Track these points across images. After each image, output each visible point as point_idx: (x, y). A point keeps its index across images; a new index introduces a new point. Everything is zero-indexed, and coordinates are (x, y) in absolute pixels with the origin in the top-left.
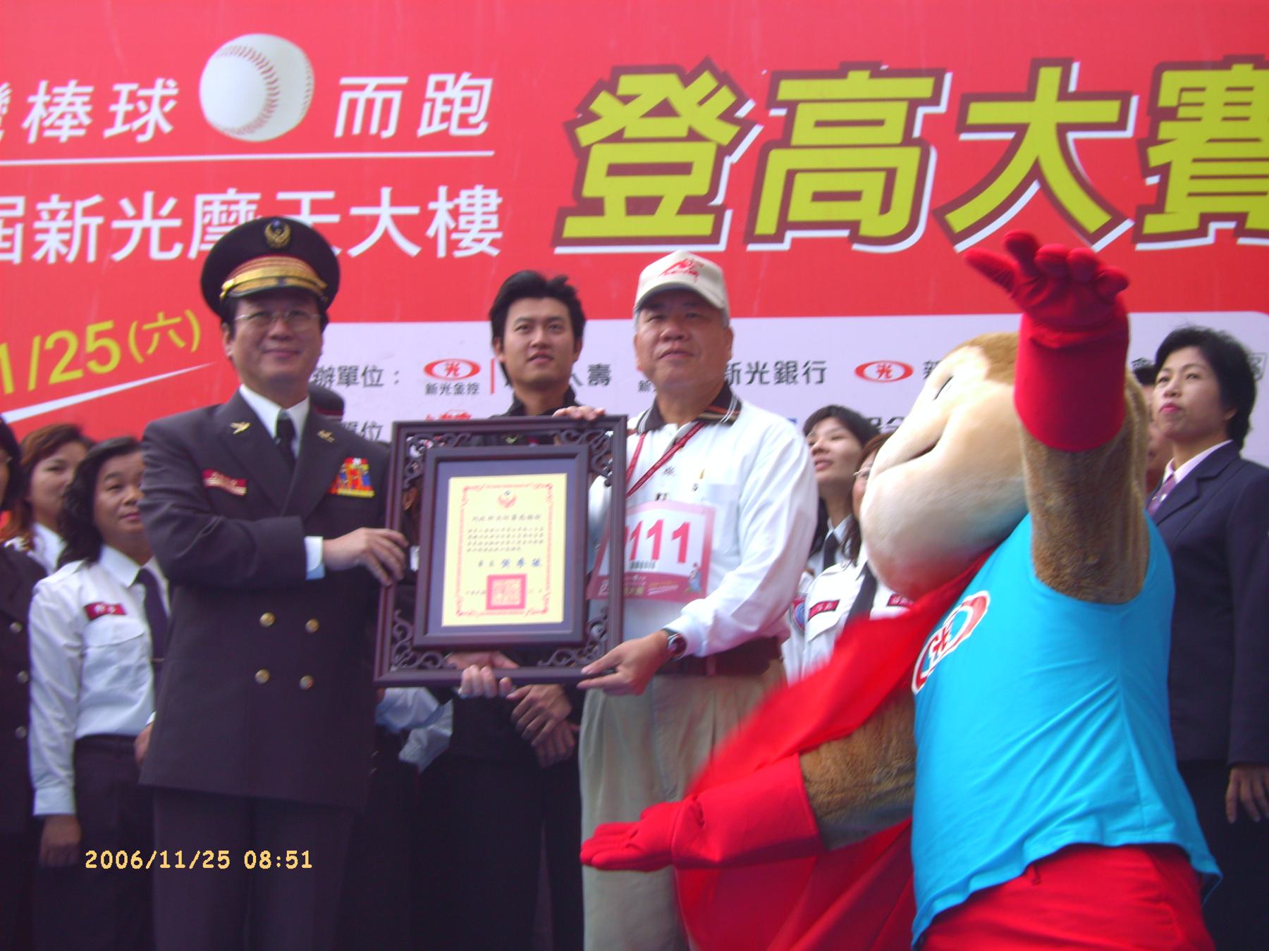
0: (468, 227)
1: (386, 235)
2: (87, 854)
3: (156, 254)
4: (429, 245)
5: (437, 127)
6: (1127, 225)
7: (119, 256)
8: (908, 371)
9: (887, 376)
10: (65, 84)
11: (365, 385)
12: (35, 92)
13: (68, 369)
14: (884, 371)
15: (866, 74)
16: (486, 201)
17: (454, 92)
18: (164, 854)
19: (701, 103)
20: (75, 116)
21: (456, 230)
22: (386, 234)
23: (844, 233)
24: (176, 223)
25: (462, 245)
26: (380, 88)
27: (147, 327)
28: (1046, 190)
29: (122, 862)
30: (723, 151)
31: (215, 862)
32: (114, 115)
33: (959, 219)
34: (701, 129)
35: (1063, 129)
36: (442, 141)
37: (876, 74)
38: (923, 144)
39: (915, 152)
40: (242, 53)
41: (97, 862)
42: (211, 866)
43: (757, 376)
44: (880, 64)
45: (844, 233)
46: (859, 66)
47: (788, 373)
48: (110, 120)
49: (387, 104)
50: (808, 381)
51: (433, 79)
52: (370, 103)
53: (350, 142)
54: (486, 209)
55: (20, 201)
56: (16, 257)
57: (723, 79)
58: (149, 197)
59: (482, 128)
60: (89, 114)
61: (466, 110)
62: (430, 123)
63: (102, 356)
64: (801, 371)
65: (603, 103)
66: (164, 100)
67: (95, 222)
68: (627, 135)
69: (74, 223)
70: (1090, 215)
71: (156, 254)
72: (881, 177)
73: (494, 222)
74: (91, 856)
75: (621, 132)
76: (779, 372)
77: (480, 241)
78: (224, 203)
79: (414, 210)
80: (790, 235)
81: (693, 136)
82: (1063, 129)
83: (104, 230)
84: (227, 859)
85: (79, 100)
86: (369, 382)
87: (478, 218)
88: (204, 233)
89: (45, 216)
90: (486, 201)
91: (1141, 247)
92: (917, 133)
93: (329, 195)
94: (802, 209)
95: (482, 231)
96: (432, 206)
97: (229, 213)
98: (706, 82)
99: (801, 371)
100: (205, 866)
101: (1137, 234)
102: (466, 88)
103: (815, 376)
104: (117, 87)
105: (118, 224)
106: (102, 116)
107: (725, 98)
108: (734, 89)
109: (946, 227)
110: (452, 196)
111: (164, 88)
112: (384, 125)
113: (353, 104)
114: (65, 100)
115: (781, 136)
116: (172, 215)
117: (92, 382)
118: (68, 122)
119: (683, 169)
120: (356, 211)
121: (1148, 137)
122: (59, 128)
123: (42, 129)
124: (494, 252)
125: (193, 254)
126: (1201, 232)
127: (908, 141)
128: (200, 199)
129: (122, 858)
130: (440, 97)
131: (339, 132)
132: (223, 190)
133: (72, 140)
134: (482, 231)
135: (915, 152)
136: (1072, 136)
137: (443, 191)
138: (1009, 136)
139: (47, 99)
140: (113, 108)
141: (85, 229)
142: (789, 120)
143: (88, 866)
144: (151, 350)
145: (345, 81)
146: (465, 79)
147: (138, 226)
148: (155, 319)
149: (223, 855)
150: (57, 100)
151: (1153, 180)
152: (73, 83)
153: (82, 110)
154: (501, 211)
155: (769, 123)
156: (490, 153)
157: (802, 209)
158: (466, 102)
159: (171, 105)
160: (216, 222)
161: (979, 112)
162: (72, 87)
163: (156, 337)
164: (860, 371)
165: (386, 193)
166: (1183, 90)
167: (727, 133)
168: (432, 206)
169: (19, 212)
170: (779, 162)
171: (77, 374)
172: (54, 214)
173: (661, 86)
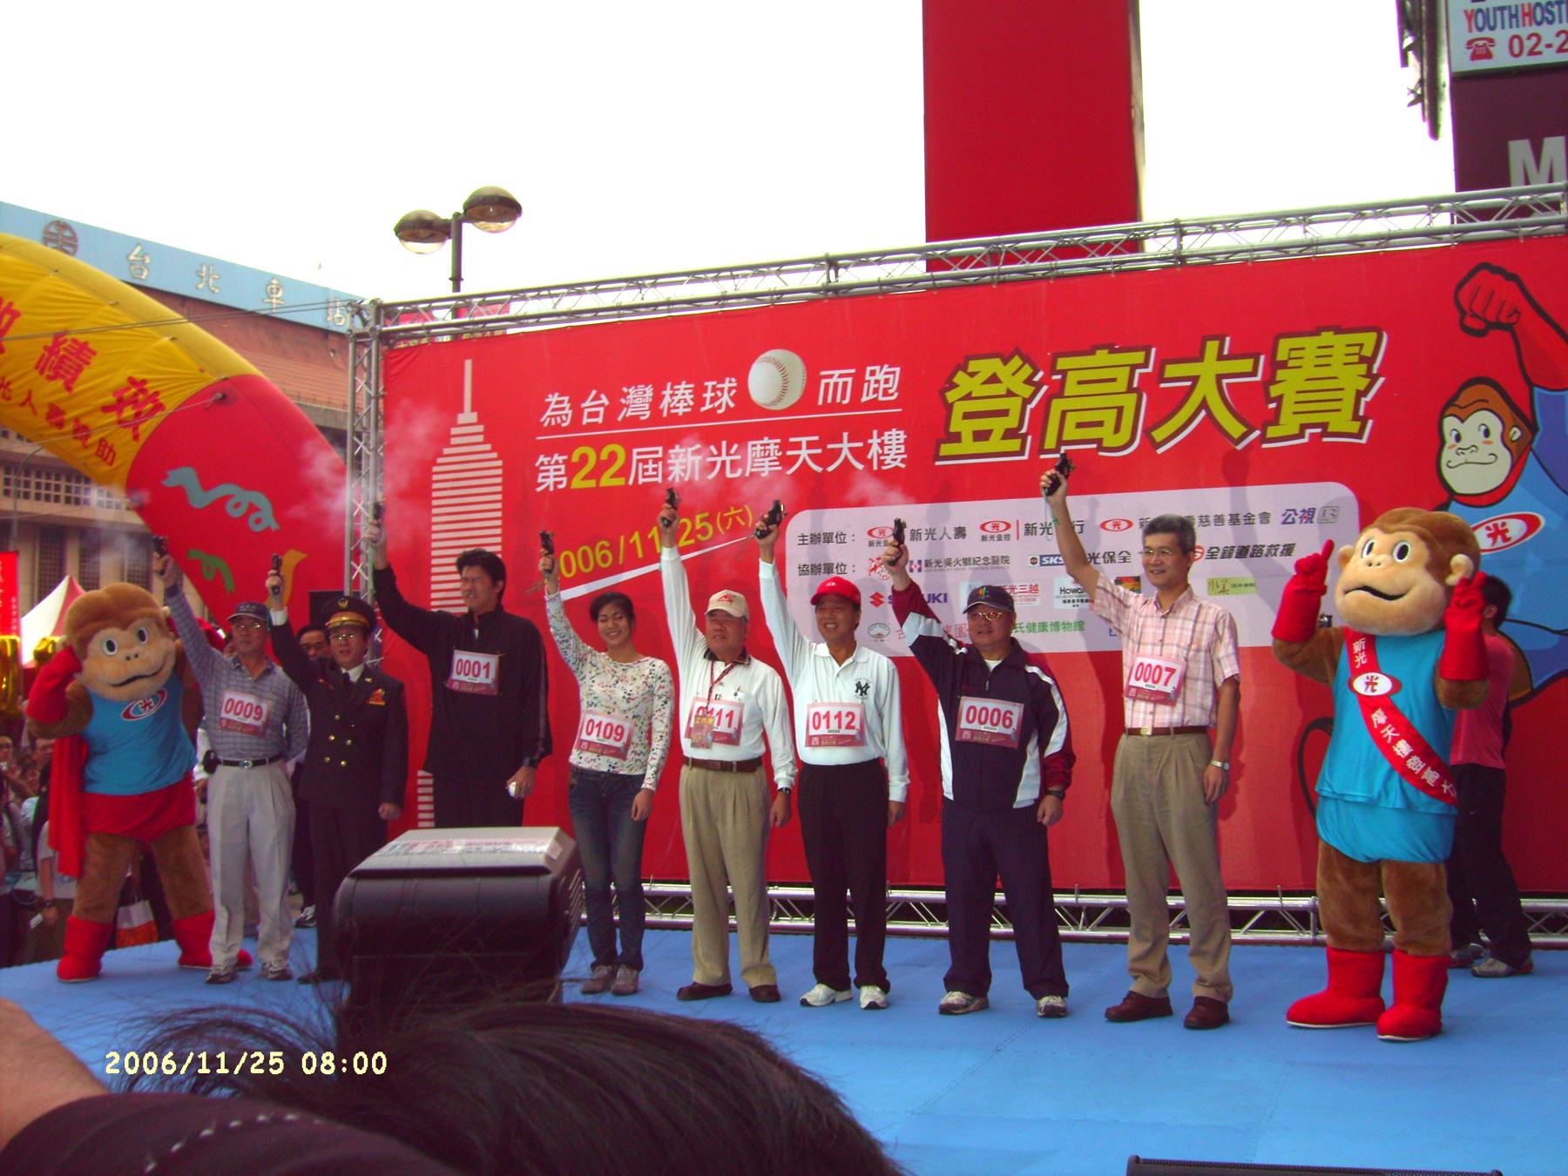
3: (729, 475)
4: (868, 463)
5: (872, 397)
6: (1257, 433)
8: (1130, 524)
10: (680, 384)
12: (665, 389)
13: (688, 538)
14: (1117, 525)
15: (1106, 351)
17: (880, 376)
19: (1014, 374)
20: (686, 401)
21: (883, 454)
22: (846, 457)
23: (1094, 446)
24: (738, 457)
26: (841, 376)
28: (1210, 415)
30: (1026, 401)
33: (1159, 435)
34: (1013, 389)
35: (1219, 378)
36: (874, 404)
37: (1112, 351)
38: (1138, 391)
39: (1134, 396)
40: (769, 360)
45: (1094, 446)
49: (845, 384)
51: (869, 369)
52: (836, 384)
53: (827, 407)
55: (660, 449)
56: (659, 479)
57: (1026, 360)
58: (724, 443)
59: (896, 395)
61: (887, 386)
62: (868, 395)
65: (960, 378)
66: (730, 389)
68: (973, 395)
70: (1234, 428)
72: (1116, 410)
73: (903, 447)
75: (970, 393)
77: (895, 460)
78: (762, 445)
79: (860, 444)
81: (1010, 394)
82: (1219, 378)
85: (687, 392)
88: (753, 462)
89: (673, 456)
91: (1265, 446)
92: (1135, 385)
93: (816, 438)
94: (1071, 433)
95: (896, 454)
96: (870, 441)
97: (765, 450)
98: (1016, 361)
101: (1263, 439)
102: (886, 373)
104: (706, 384)
106: (699, 401)
107: (1027, 370)
108: (1032, 365)
109: (1152, 440)
110: (879, 437)
111: (729, 383)
112: (843, 397)
113: (827, 385)
114: (680, 392)
115: (1058, 391)
119: (1004, 413)
120: (830, 446)
121: (1270, 379)
122: (678, 408)
123: (669, 409)
124: (903, 466)
126: (1301, 436)
127: (1130, 390)
130: (872, 379)
131: (820, 403)
134: (896, 454)
135: (1134, 396)
136: (1225, 381)
137: (875, 433)
138: (1189, 383)
139: (671, 392)
140: (705, 395)
142: (1063, 382)
145: (823, 373)
146: (886, 368)
147: (719, 460)
148: (730, 511)
151: (1272, 406)
153: (689, 397)
154: (906, 442)
156: (900, 410)
157: (1071, 433)
158: (887, 381)
159: (734, 392)
161: (1172, 370)
162: (684, 385)
163: (730, 520)
165: (845, 435)
167: (1027, 391)
168: (870, 441)
169: (660, 455)
170: (1057, 406)
171: (692, 542)
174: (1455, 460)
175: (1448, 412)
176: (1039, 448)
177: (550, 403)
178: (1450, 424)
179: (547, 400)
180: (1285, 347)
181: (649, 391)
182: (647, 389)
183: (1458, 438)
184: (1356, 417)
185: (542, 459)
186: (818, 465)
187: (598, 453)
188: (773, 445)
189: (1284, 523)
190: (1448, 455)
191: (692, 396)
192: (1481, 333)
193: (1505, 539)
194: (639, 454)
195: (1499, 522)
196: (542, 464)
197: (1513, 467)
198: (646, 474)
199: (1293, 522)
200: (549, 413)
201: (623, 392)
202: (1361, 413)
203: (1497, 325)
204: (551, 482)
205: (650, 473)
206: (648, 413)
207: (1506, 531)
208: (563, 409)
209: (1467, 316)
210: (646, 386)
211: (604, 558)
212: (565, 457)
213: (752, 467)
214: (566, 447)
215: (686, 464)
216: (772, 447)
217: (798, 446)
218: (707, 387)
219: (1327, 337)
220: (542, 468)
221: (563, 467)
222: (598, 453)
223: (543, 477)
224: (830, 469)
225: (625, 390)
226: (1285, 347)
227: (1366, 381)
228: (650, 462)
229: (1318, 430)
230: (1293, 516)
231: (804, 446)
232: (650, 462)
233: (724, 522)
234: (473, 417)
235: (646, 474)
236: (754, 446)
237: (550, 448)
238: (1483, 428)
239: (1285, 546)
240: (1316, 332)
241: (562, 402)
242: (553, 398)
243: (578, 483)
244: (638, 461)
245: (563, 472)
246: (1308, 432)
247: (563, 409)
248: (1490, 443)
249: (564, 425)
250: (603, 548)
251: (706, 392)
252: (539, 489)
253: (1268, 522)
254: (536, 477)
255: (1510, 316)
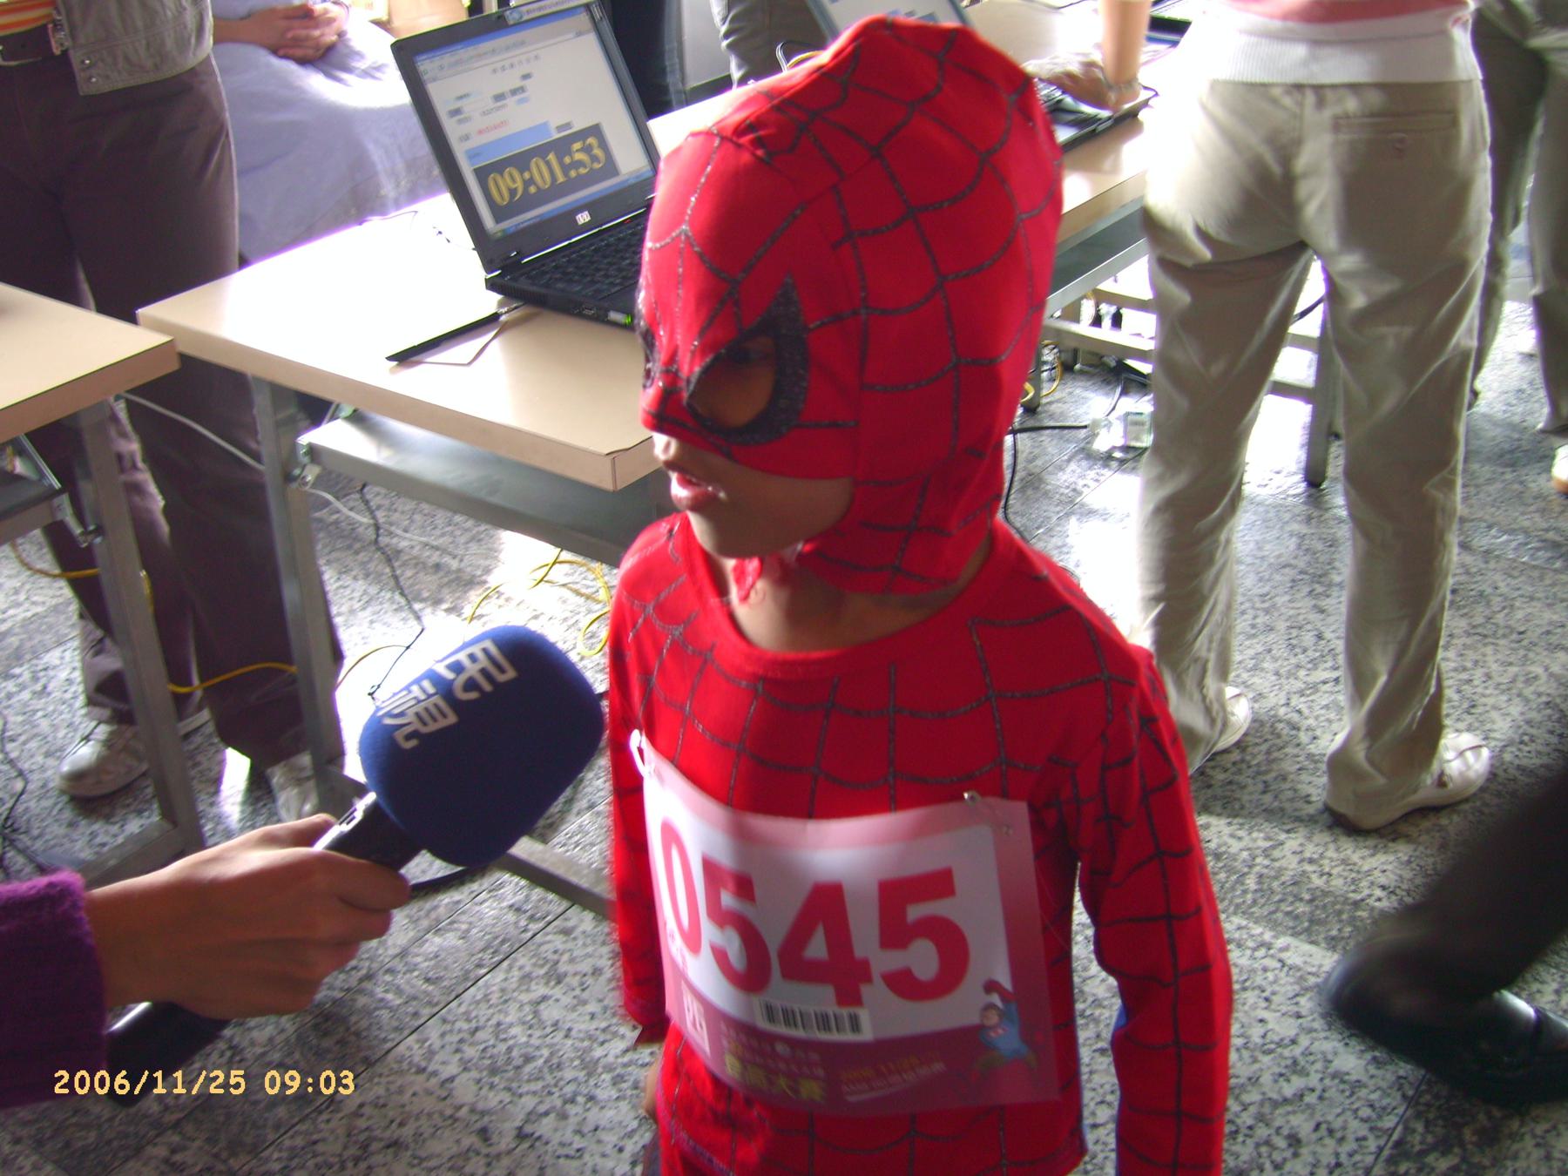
2: (56, 1075)
18: (159, 1074)
29: (102, 1085)
31: (226, 1085)
41: (70, 1085)
42: (221, 1091)
74: (62, 1077)
84: (242, 1081)
100: (213, 1090)
129: (102, 1080)
143: (57, 1090)
149: (236, 1076)
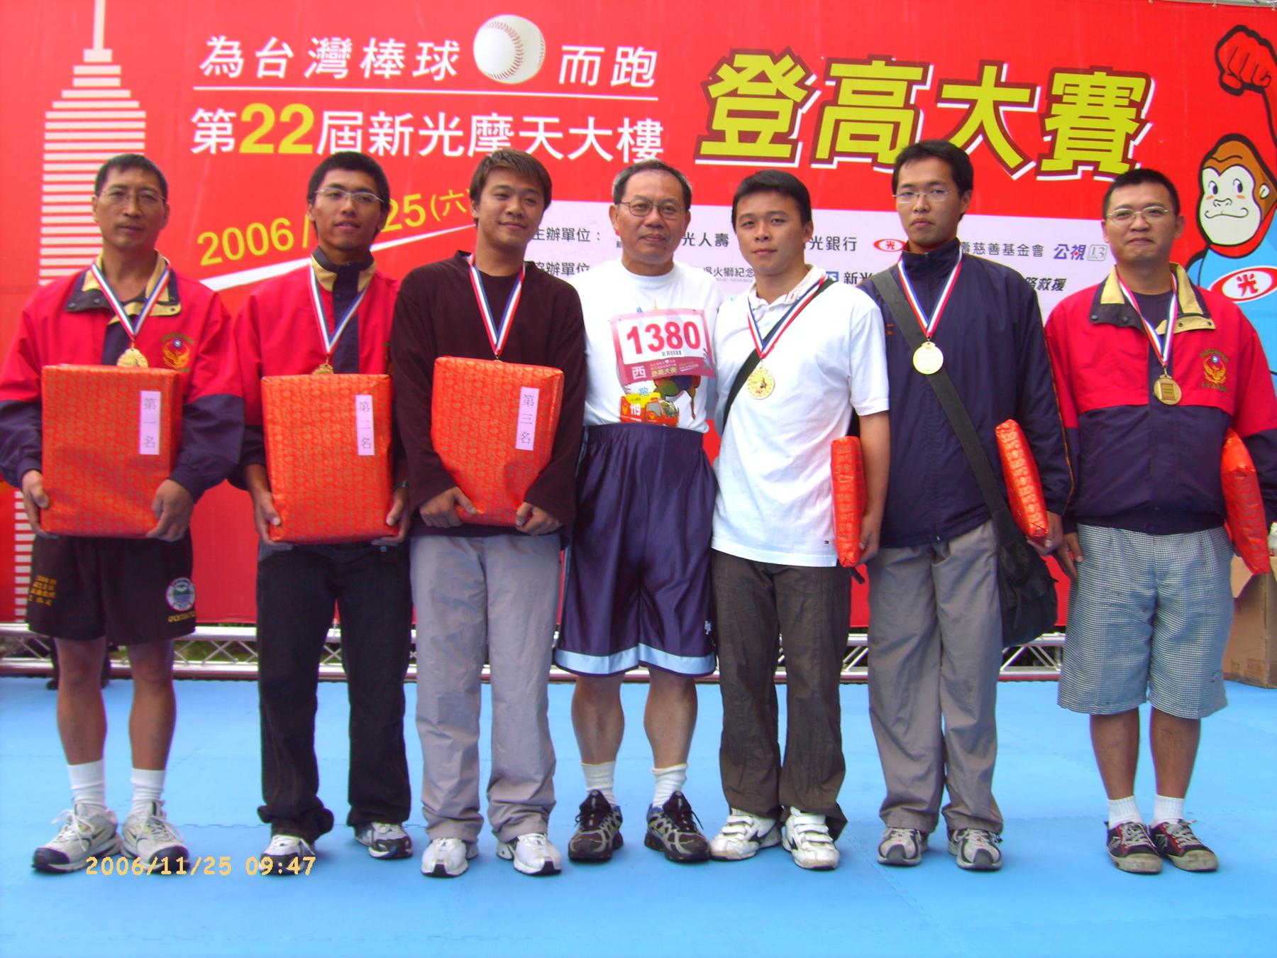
0: (642, 144)
1: (592, 147)
4: (618, 155)
5: (623, 81)
6: (1032, 165)
7: (424, 153)
9: (893, 248)
10: (387, 41)
11: (579, 240)
12: (368, 45)
15: (884, 62)
16: (653, 129)
17: (634, 59)
19: (784, 75)
20: (394, 62)
21: (635, 146)
22: (592, 145)
23: (869, 160)
24: (460, 133)
25: (639, 155)
26: (587, 54)
27: (442, 198)
28: (986, 140)
32: (418, 63)
35: (997, 104)
37: (889, 63)
38: (915, 108)
39: (911, 113)
40: (500, 26)
43: (816, 244)
44: (891, 57)
45: (869, 160)
46: (879, 58)
47: (834, 243)
48: (416, 66)
49: (592, 64)
50: (846, 249)
51: (620, 50)
52: (581, 63)
53: (568, 87)
54: (653, 134)
55: (360, 115)
56: (358, 150)
57: (797, 61)
58: (442, 116)
60: (402, 61)
62: (619, 78)
63: (414, 215)
64: (842, 242)
65: (725, 71)
66: (451, 55)
67: (408, 130)
68: (739, 92)
69: (394, 131)
70: (1012, 158)
71: (447, 152)
72: (892, 126)
75: (736, 90)
76: (829, 243)
78: (489, 122)
79: (609, 133)
80: (836, 160)
81: (780, 95)
82: (997, 104)
83: (414, 136)
85: (396, 52)
86: (581, 238)
87: (648, 139)
88: (478, 140)
89: (376, 125)
90: (653, 129)
91: (1040, 178)
92: (912, 101)
93: (556, 120)
94: (844, 144)
95: (651, 147)
96: (620, 130)
97: (493, 128)
98: (787, 62)
99: (842, 242)
101: (1037, 171)
102: (641, 57)
103: (850, 246)
104: (421, 45)
105: (422, 133)
106: (411, 63)
107: (799, 73)
108: (804, 67)
110: (632, 124)
111: (450, 47)
112: (590, 77)
113: (570, 63)
115: (831, 98)
116: (457, 128)
117: (408, 232)
118: (389, 65)
119: (773, 115)
120: (572, 131)
121: (1046, 113)
122: (384, 69)
123: (373, 69)
125: (471, 154)
126: (1074, 172)
127: (907, 106)
128: (475, 119)
130: (624, 61)
131: (562, 80)
132: (490, 114)
133: (393, 77)
134: (651, 147)
135: (911, 113)
136: (1002, 109)
137: (626, 121)
138: (966, 106)
139: (376, 50)
140: (418, 58)
141: (402, 135)
142: (837, 89)
144: (445, 214)
145: (565, 48)
146: (640, 51)
148: (448, 194)
150: (382, 51)
151: (1047, 139)
152: (392, 41)
153: (399, 59)
154: (663, 135)
155: (825, 90)
156: (656, 99)
157: (844, 144)
158: (641, 66)
159: (455, 58)
160: (485, 134)
161: (949, 91)
162: (392, 43)
163: (448, 205)
164: (877, 245)
165: (591, 121)
166: (1066, 85)
167: (799, 94)
168: (620, 130)
169: (360, 122)
170: (830, 114)
171: (398, 227)
172: (381, 124)
173: (759, 63)
174: (1214, 211)
175: (1206, 165)
176: (810, 156)
177: (212, 49)
178: (1208, 175)
179: (210, 44)
180: (1060, 80)
181: (347, 46)
182: (343, 43)
183: (1215, 190)
184: (1125, 159)
185: (201, 113)
186: (558, 150)
187: (278, 114)
188: (503, 123)
189: (1056, 257)
190: (1206, 205)
191: (402, 57)
192: (1237, 93)
193: (1254, 291)
194: (331, 118)
195: (1248, 274)
196: (202, 120)
197: (1262, 222)
198: (340, 142)
199: (1065, 257)
200: (212, 59)
201: (313, 44)
202: (1130, 156)
203: (1251, 87)
204: (212, 143)
205: (347, 142)
206: (345, 73)
207: (1254, 282)
208: (232, 56)
209: (1226, 73)
210: (344, 39)
211: (283, 240)
212: (233, 115)
213: (477, 146)
214: (235, 103)
215: (392, 135)
216: (502, 126)
217: (534, 127)
218: (421, 49)
219: (1100, 77)
220: (201, 125)
221: (229, 126)
222: (278, 114)
223: (203, 136)
224: (573, 156)
225: (315, 41)
226: (1060, 80)
227: (1136, 125)
228: (347, 129)
229: (1090, 168)
230: (1065, 251)
231: (541, 127)
232: (347, 129)
233: (440, 206)
234: (107, 55)
235: (340, 142)
236: (480, 122)
237: (212, 103)
238: (1237, 183)
239: (1056, 280)
240: (1090, 71)
241: (230, 48)
242: (218, 43)
243: (250, 146)
244: (331, 127)
245: (229, 132)
246: (1081, 169)
247: (232, 56)
248: (1242, 197)
249: (232, 75)
250: (281, 226)
251: (420, 54)
252: (196, 151)
253: (1041, 255)
254: (193, 136)
255: (1262, 79)
